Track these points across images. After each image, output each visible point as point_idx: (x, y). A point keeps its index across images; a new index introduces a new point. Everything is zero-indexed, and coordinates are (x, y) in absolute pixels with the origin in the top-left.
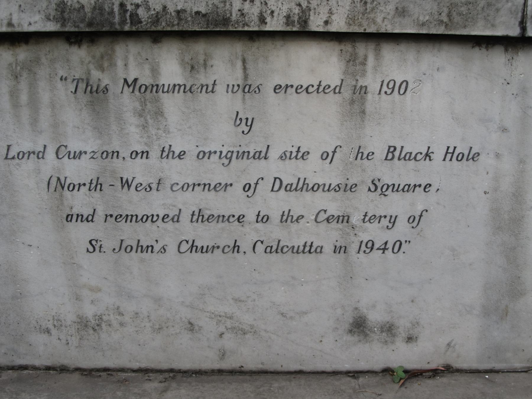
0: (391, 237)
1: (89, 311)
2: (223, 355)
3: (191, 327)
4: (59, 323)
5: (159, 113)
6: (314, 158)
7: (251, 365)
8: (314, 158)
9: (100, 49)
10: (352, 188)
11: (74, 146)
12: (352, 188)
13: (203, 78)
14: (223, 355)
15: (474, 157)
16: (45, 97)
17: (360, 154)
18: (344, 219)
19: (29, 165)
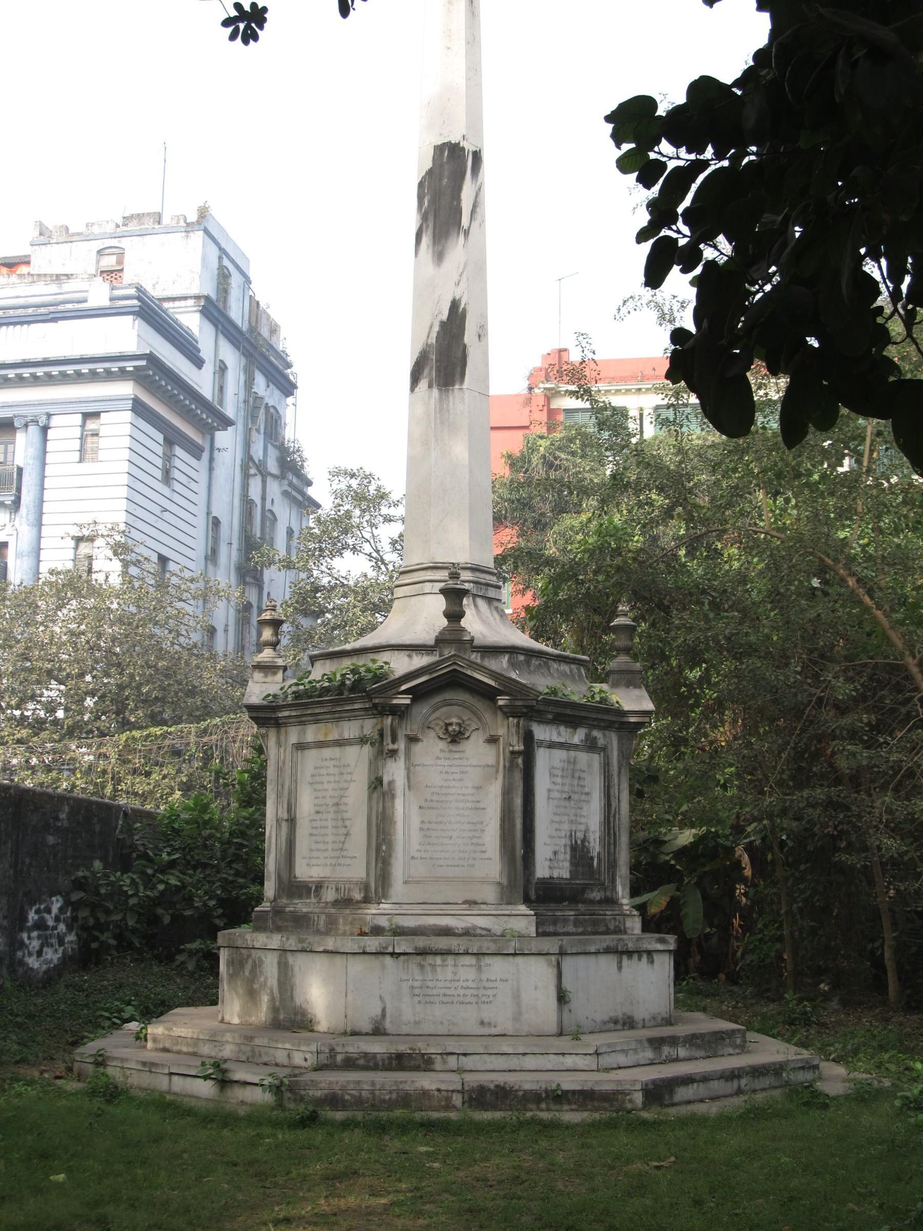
0: (488, 1000)
1: (417, 1019)
2: (449, 1030)
3: (442, 1023)
4: (409, 1022)
5: (436, 971)
6: (470, 982)
7: (456, 1033)
8: (470, 982)
9: (424, 956)
10: (479, 988)
11: (416, 978)
12: (479, 988)
13: (446, 963)
14: (449, 1030)
15: (507, 981)
16: (410, 966)
17: (481, 980)
18: (478, 996)
19: (405, 983)
